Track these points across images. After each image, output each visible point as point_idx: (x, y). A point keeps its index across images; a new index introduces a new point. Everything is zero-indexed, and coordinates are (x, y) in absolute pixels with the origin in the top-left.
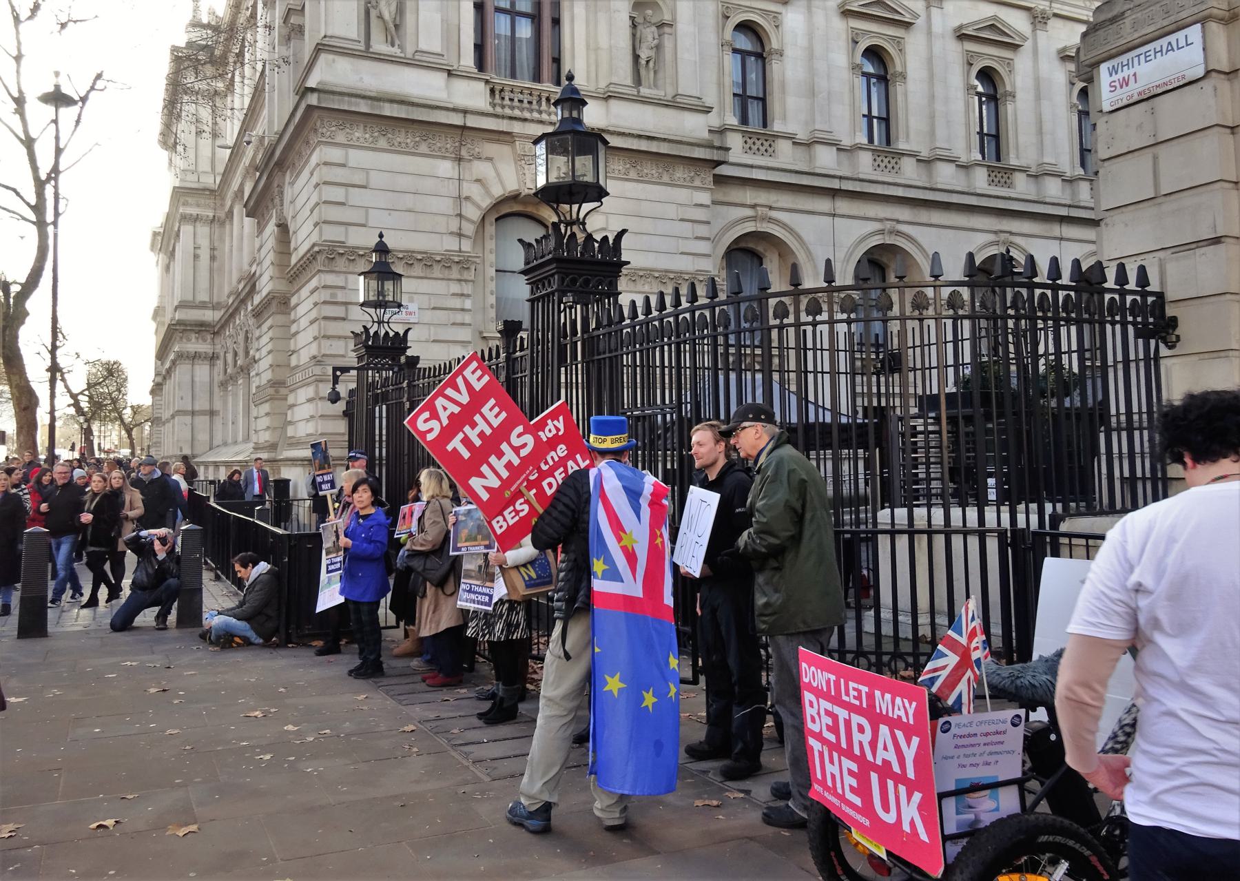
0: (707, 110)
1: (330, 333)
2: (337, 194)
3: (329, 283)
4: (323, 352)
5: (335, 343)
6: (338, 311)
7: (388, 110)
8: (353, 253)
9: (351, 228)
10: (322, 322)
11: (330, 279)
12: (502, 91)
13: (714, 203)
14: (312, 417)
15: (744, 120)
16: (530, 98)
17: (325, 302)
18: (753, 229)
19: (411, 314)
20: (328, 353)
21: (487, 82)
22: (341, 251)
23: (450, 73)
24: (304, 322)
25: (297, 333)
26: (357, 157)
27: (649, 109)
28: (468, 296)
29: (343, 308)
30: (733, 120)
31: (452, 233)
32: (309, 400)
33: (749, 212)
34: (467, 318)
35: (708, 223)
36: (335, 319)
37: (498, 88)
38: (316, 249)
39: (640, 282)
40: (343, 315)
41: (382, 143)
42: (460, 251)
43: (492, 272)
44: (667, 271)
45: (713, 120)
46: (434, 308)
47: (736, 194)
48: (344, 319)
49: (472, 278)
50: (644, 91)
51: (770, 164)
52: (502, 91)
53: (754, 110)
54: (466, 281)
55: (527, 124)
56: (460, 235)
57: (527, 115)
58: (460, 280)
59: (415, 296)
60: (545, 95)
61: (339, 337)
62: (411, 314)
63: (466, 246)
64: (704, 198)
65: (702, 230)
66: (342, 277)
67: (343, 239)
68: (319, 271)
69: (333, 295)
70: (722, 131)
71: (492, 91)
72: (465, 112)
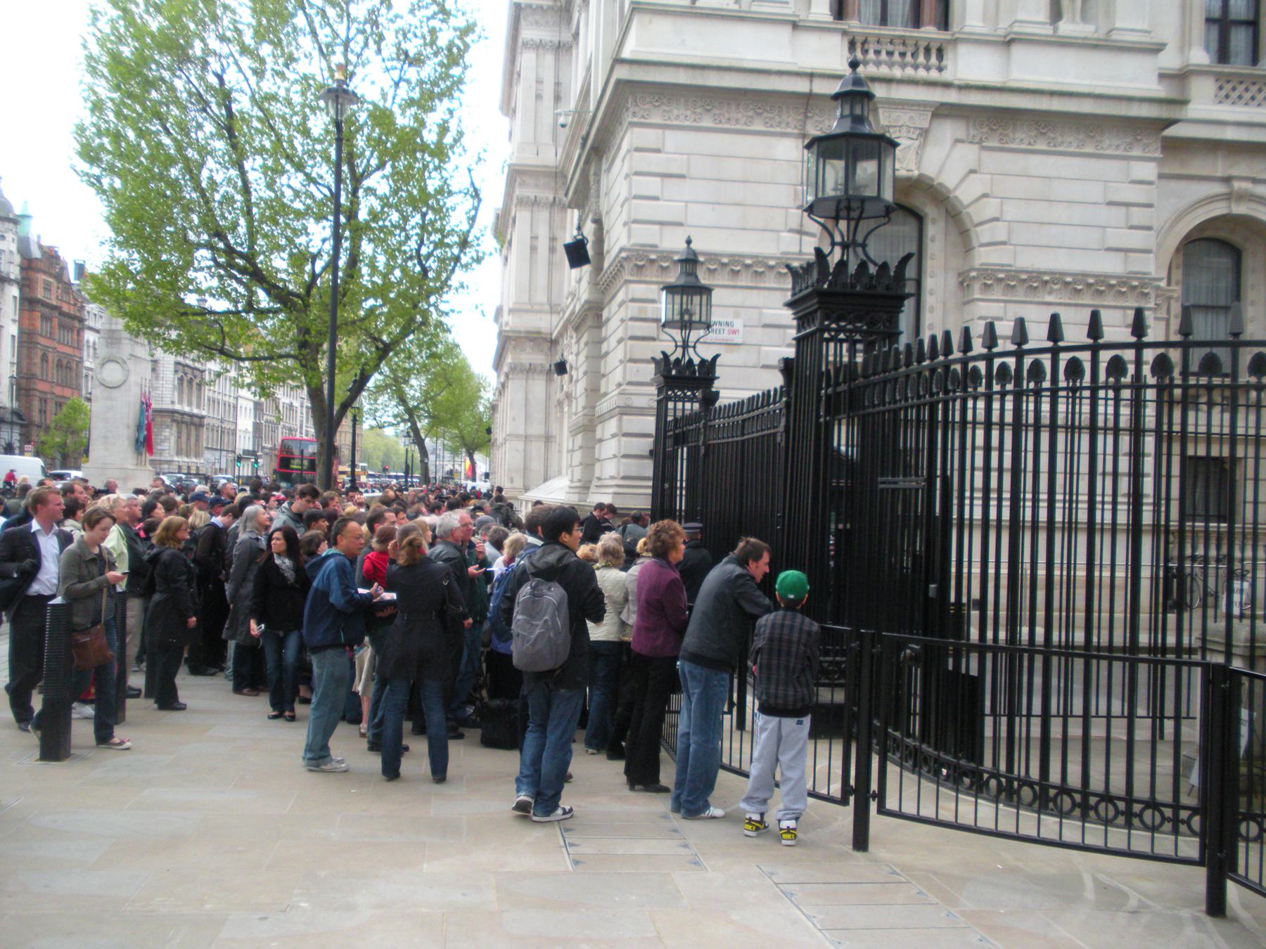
0: (1157, 49)
1: (636, 356)
2: (652, 186)
3: (638, 296)
4: (628, 379)
7: (713, 80)
9: (667, 229)
10: (630, 343)
12: (863, 43)
13: (1161, 176)
14: (615, 456)
15: (1223, 54)
16: (901, 49)
17: (632, 319)
18: (1224, 211)
19: (734, 332)
20: (634, 379)
21: (844, 33)
22: (653, 256)
23: (795, 26)
24: (613, 341)
25: (607, 353)
26: (673, 139)
27: (1070, 56)
30: (1200, 56)
31: (791, 231)
32: (614, 436)
33: (1218, 188)
35: (1150, 206)
37: (859, 40)
38: (624, 255)
41: (707, 122)
42: (800, 252)
44: (1085, 275)
45: (1170, 60)
46: (765, 326)
47: (1199, 165)
50: (1067, 28)
51: (1256, 119)
52: (863, 43)
53: (1240, 39)
55: (894, 87)
56: (801, 232)
57: (897, 72)
59: (742, 310)
60: (923, 44)
62: (734, 332)
64: (1148, 170)
65: (1138, 216)
68: (627, 282)
69: (641, 310)
70: (1181, 77)
71: (852, 45)
72: (811, 76)
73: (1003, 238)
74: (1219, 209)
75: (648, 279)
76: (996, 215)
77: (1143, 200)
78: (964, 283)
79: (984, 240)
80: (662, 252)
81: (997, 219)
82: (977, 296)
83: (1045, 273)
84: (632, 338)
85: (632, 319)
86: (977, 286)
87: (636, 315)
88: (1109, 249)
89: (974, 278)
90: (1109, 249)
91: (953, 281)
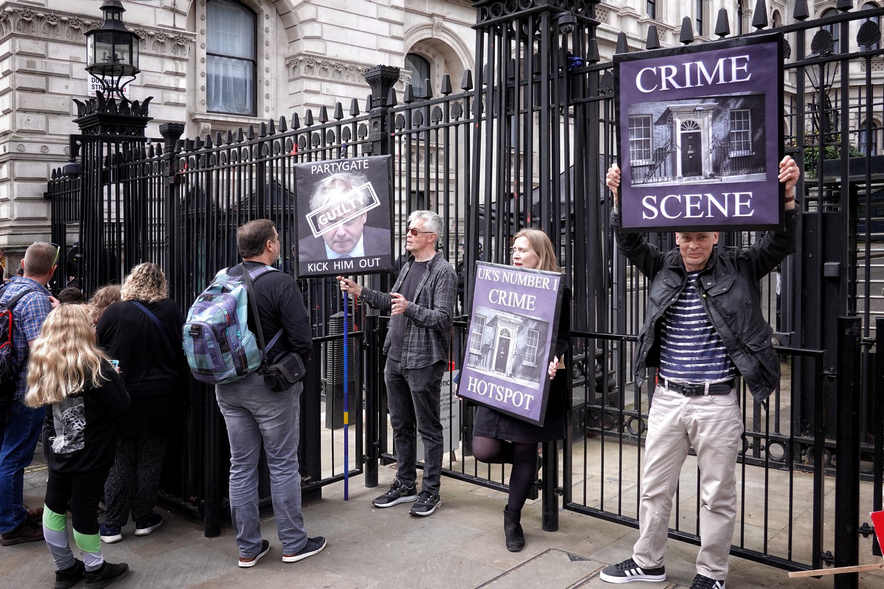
3: (25, 49)
4: (18, 127)
5: (33, 117)
6: (37, 82)
8: (55, 18)
10: (18, 93)
11: (27, 45)
17: (20, 71)
22: (41, 14)
28: (183, 75)
29: (44, 78)
33: (426, 21)
34: (182, 98)
36: (33, 90)
38: (9, 9)
39: (345, 74)
40: (43, 87)
42: (174, 27)
43: (202, 53)
48: (43, 91)
49: (187, 57)
54: (181, 60)
58: (174, 59)
61: (39, 112)
63: (182, 23)
65: (398, 31)
66: (42, 44)
67: (43, 2)
68: (12, 35)
73: (318, 34)
74: (427, 34)
75: (34, 34)
76: (315, 17)
77: (399, 19)
78: (292, 63)
79: (308, 34)
80: (50, 11)
81: (314, 20)
82: (304, 75)
83: (346, 62)
84: (20, 89)
85: (20, 71)
86: (302, 67)
87: (24, 67)
88: (381, 50)
89: (301, 61)
90: (381, 50)
91: (281, 64)
